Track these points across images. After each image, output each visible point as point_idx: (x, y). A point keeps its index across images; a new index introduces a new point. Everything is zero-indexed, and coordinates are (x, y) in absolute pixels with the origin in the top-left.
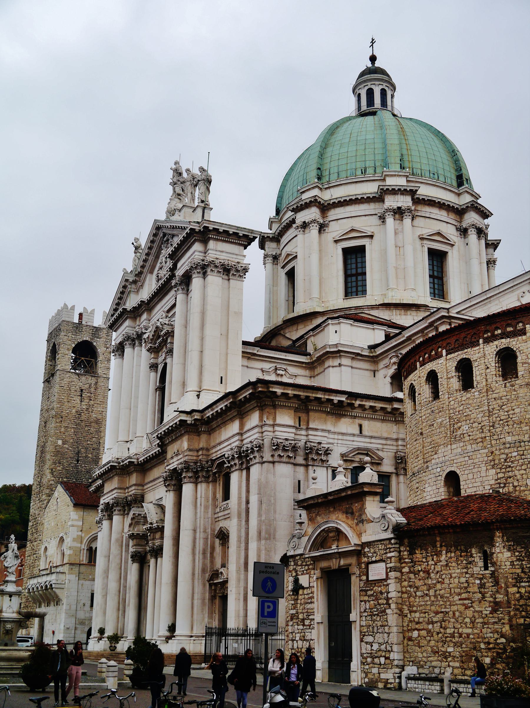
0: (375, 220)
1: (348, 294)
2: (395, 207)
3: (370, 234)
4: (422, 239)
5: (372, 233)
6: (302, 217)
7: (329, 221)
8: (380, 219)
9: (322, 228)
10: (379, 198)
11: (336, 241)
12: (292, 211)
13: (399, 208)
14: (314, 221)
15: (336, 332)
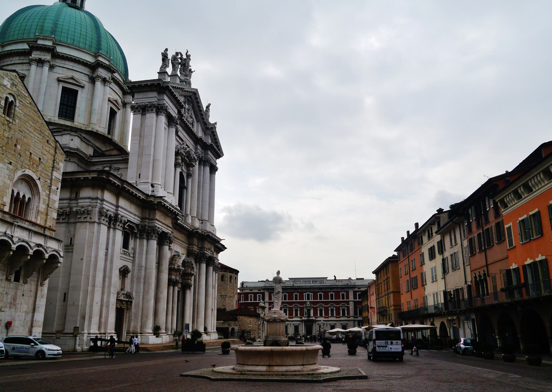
0: (86, 79)
1: (61, 116)
2: (104, 77)
3: (82, 85)
4: (109, 100)
5: (85, 85)
6: (35, 55)
7: (56, 66)
8: (89, 79)
9: (52, 67)
10: (93, 67)
11: (59, 80)
12: (29, 46)
13: (105, 78)
14: (49, 62)
15: (72, 140)
